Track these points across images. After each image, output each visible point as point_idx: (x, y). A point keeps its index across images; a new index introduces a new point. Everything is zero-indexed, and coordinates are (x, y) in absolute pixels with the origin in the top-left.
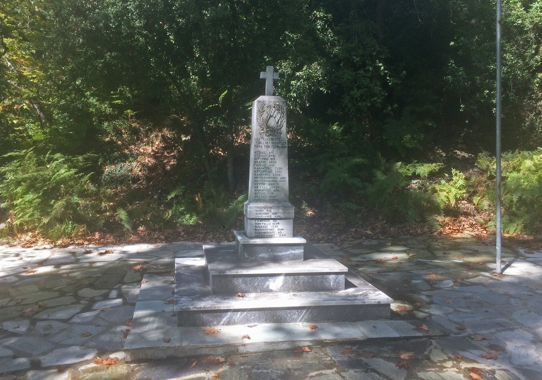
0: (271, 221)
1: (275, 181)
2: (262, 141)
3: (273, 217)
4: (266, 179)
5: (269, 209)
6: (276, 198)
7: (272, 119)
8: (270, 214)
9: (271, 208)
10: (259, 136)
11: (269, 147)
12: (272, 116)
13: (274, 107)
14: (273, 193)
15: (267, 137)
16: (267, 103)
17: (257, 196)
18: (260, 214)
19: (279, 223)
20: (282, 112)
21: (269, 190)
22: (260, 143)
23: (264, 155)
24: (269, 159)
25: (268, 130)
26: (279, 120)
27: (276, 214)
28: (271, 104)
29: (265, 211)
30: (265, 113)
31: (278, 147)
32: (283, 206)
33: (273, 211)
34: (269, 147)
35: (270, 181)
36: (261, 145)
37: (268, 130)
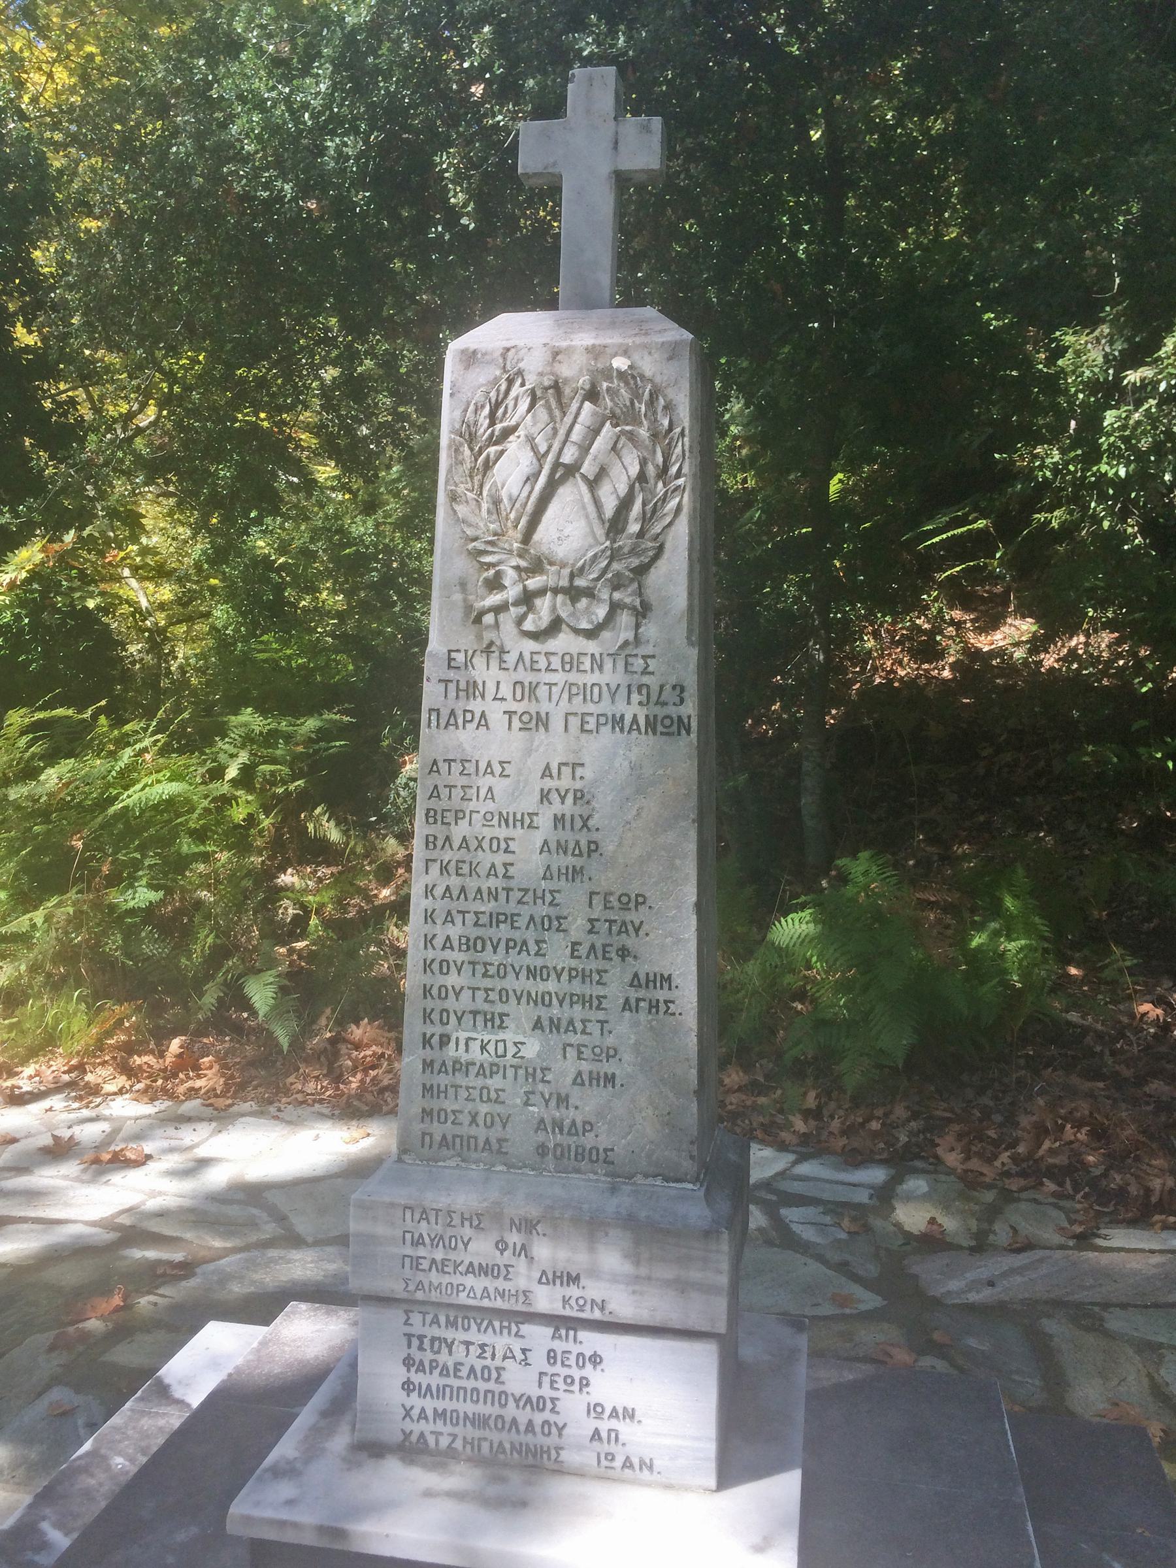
0: (539, 1337)
1: (583, 1000)
2: (484, 672)
3: (546, 1300)
4: (510, 983)
5: (514, 1238)
6: (588, 1140)
7: (570, 495)
8: (523, 1277)
9: (528, 1226)
10: (466, 640)
11: (542, 721)
12: (571, 470)
13: (592, 395)
14: (563, 1100)
15: (530, 645)
16: (534, 365)
17: (441, 1116)
18: (440, 1266)
19: (596, 1360)
20: (655, 436)
21: (534, 1073)
22: (472, 689)
23: (501, 786)
24: (544, 821)
25: (533, 583)
26: (625, 504)
27: (573, 1279)
28: (566, 370)
29: (482, 1248)
30: (513, 445)
31: (617, 722)
32: (629, 1222)
33: (543, 1251)
34: (542, 721)
35: (543, 1000)
36: (476, 706)
37: (533, 583)
